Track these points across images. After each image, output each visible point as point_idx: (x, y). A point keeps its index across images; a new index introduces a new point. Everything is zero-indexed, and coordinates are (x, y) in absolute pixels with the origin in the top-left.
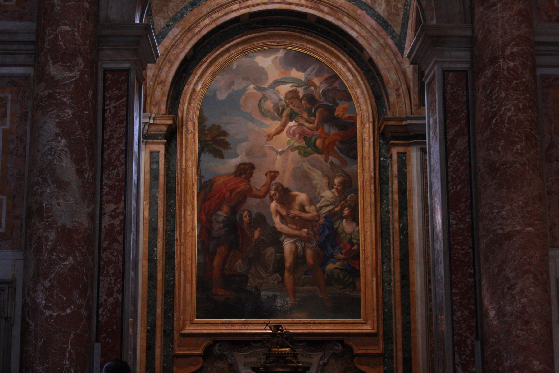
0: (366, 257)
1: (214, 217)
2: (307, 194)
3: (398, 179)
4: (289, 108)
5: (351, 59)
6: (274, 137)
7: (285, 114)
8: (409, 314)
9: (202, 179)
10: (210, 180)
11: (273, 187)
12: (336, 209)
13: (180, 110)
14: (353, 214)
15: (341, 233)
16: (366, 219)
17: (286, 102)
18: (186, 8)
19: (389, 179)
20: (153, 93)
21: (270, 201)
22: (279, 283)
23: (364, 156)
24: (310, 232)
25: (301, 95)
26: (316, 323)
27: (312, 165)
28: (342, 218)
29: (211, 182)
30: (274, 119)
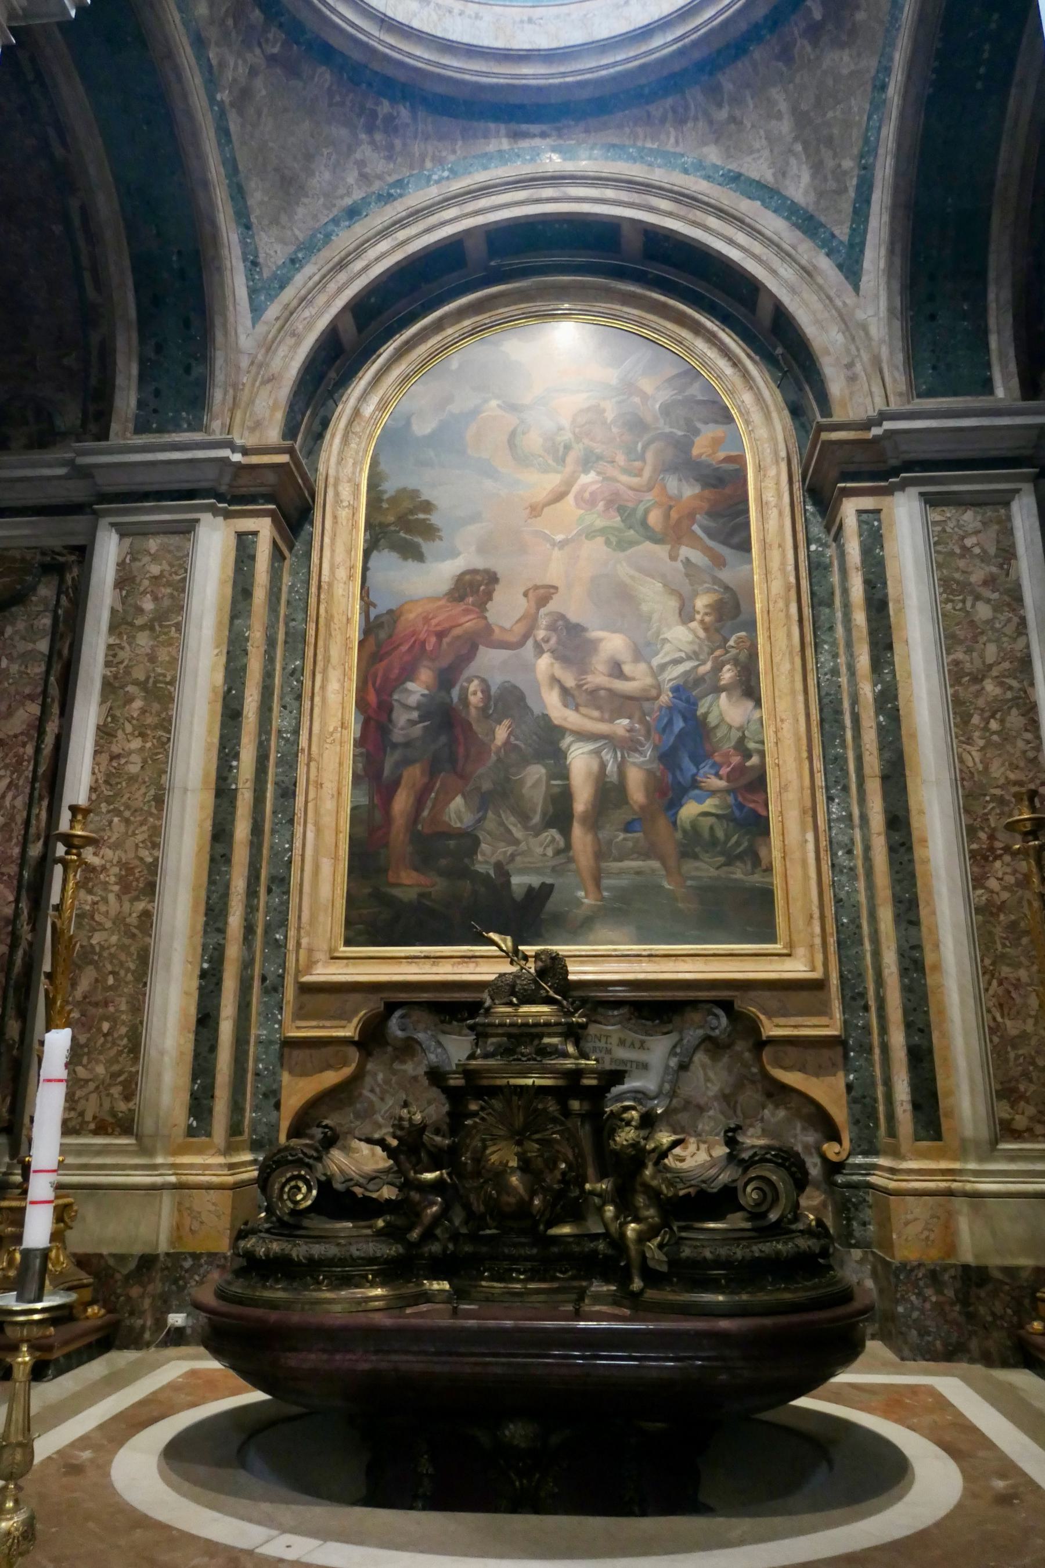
0: (783, 784)
1: (396, 697)
3: (864, 574)
4: (581, 446)
5: (727, 330)
6: (546, 510)
7: (570, 459)
8: (915, 923)
9: (372, 609)
10: (390, 612)
11: (543, 622)
13: (323, 455)
16: (780, 691)
17: (574, 434)
18: (335, 221)
19: (833, 594)
20: (251, 401)
21: (535, 656)
22: (558, 852)
23: (768, 541)
25: (610, 416)
27: (641, 570)
28: (718, 690)
29: (394, 615)
30: (545, 470)
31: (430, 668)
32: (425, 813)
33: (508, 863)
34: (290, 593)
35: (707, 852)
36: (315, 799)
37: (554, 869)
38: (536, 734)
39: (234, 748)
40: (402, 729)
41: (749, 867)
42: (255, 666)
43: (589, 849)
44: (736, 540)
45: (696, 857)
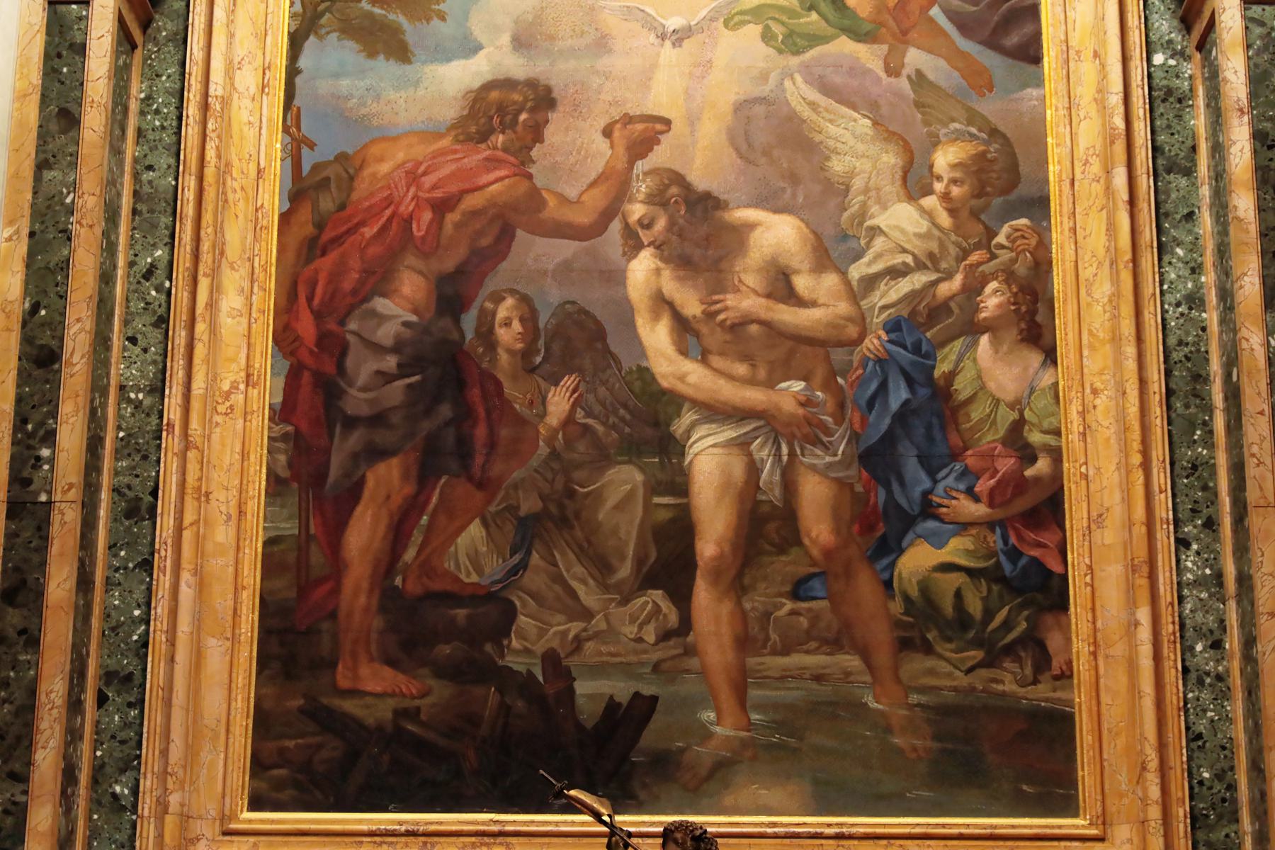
0: (1094, 514)
1: (353, 326)
2: (802, 220)
3: (1252, 122)
9: (305, 151)
10: (342, 158)
11: (642, 188)
12: (945, 289)
14: (1024, 309)
15: (970, 400)
16: (1090, 333)
19: (1194, 149)
21: (624, 254)
22: (665, 636)
24: (819, 393)
26: (851, 837)
28: (973, 329)
31: (420, 273)
32: (410, 555)
33: (568, 656)
34: (142, 113)
35: (949, 640)
36: (196, 522)
37: (656, 668)
38: (625, 406)
39: (42, 423)
40: (364, 389)
41: (1028, 671)
42: (85, 262)
43: (726, 633)
44: (1013, 40)
45: (928, 649)
